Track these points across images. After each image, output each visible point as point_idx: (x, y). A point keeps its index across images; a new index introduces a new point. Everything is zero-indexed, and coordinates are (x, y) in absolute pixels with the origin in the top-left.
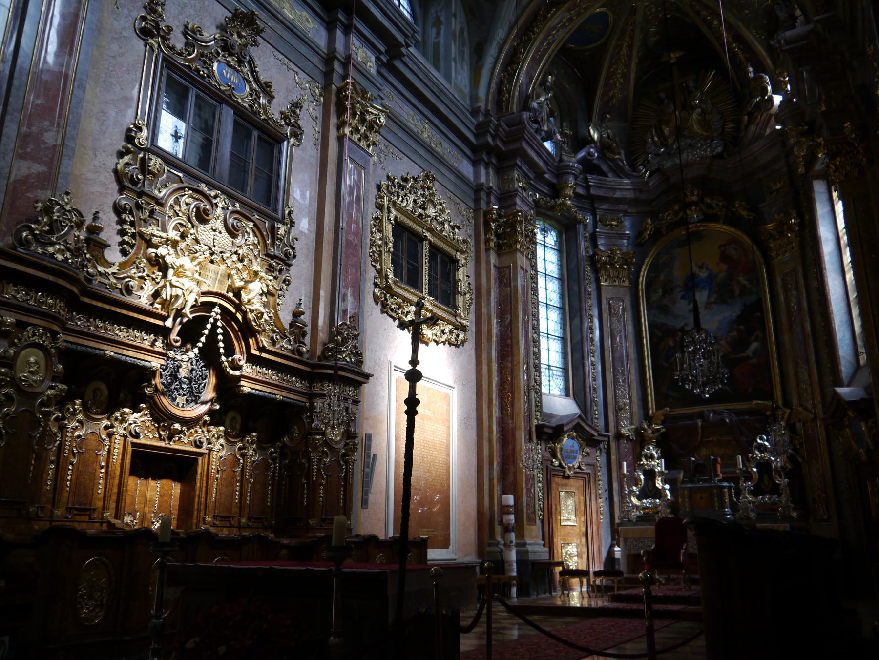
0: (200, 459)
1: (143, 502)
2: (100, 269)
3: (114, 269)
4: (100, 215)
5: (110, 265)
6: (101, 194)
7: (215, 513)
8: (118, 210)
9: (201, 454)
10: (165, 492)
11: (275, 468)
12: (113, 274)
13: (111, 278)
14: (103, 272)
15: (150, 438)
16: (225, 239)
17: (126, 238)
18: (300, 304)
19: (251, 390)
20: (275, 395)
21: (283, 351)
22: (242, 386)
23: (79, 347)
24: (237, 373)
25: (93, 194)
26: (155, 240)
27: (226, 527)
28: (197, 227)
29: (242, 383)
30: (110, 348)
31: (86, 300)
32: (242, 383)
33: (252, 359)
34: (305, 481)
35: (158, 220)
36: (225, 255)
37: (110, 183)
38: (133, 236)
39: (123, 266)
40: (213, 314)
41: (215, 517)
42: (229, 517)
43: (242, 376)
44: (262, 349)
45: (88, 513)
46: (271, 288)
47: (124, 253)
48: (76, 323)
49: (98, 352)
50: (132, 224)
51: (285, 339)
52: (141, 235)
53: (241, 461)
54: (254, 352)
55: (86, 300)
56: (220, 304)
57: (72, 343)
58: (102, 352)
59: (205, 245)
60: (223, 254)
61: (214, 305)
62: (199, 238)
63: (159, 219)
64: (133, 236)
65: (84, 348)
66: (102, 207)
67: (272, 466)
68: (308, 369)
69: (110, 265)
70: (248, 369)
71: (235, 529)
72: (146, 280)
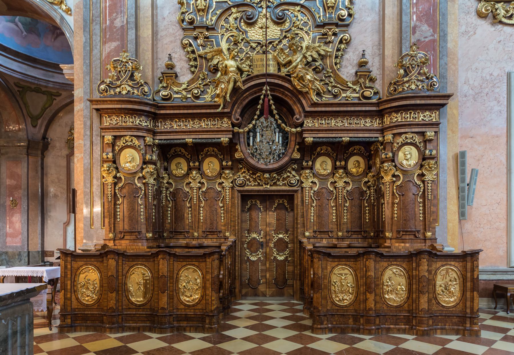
0: (295, 194)
1: (265, 224)
2: (175, 89)
3: (184, 86)
4: (173, 55)
5: (181, 85)
6: (171, 42)
7: (314, 229)
8: (184, 47)
9: (296, 191)
10: (280, 218)
11: (370, 192)
12: (183, 89)
13: (184, 93)
14: (177, 91)
15: (252, 187)
16: (274, 31)
17: (191, 64)
18: (363, 55)
19: (315, 139)
20: (341, 138)
21: (347, 100)
22: (305, 138)
23: (181, 141)
24: (299, 129)
25: (166, 44)
26: (209, 56)
27: (326, 238)
28: (246, 32)
29: (304, 136)
30: (189, 136)
31: (162, 112)
32: (304, 136)
33: (309, 114)
34: (421, 200)
35: (213, 41)
36: (275, 44)
37: (177, 32)
38: (195, 59)
39: (190, 83)
40: (264, 92)
41: (315, 232)
42: (328, 232)
43: (303, 131)
44: (315, 105)
45: (216, 233)
46: (323, 53)
47: (193, 73)
48: (164, 127)
49: (181, 141)
50: (193, 52)
51: (348, 90)
52: (200, 56)
53: (335, 192)
54: (308, 109)
55: (162, 112)
56: (268, 82)
57: (165, 140)
58: (184, 140)
59: (255, 43)
60: (273, 44)
61: (263, 84)
62: (248, 40)
63: (214, 40)
64: (195, 59)
65: (172, 141)
66: (173, 50)
67: (368, 192)
68: (374, 109)
69: (181, 85)
70: (309, 123)
71: (334, 239)
72: (209, 85)
